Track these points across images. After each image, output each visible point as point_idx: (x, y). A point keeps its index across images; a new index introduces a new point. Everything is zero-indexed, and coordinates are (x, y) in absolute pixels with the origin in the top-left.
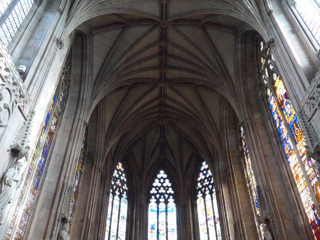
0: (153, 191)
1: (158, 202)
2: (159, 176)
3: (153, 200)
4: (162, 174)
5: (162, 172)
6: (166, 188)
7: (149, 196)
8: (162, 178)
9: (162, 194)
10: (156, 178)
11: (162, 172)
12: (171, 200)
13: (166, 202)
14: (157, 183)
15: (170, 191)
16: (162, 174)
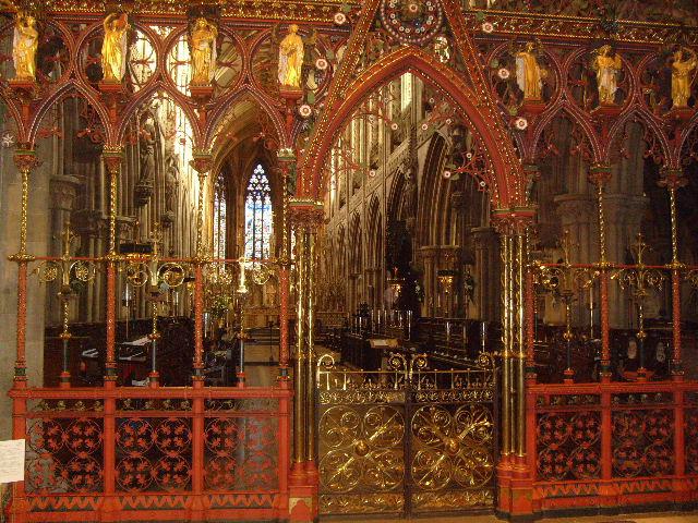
0: (250, 188)
1: (255, 200)
2: (256, 171)
3: (250, 198)
4: (259, 169)
5: (260, 166)
6: (263, 185)
7: (247, 193)
8: (259, 173)
9: (259, 191)
10: (253, 173)
11: (260, 166)
12: (268, 199)
13: (263, 199)
14: (254, 179)
15: (267, 188)
16: (259, 169)
